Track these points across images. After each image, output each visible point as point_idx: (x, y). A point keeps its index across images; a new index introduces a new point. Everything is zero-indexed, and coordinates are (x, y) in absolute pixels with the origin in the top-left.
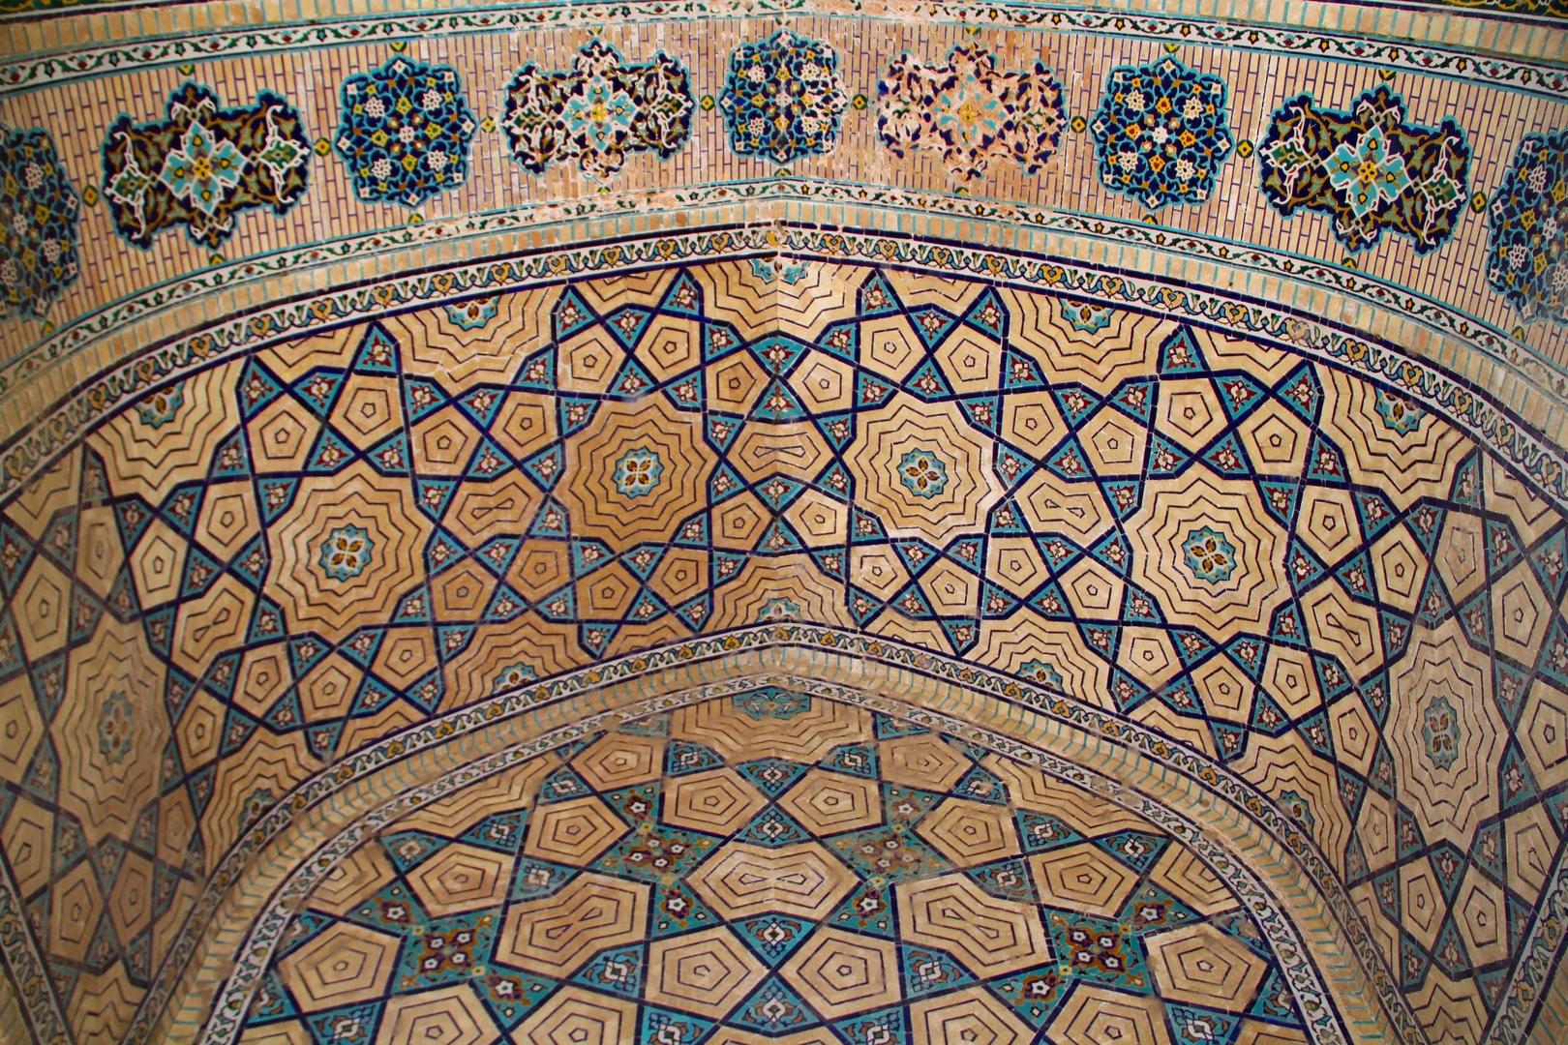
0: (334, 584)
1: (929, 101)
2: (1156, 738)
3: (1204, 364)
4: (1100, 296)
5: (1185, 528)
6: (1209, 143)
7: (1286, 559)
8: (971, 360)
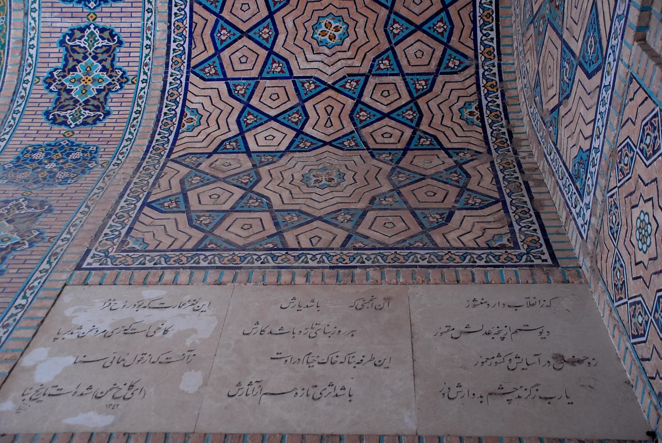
0: (347, 42)
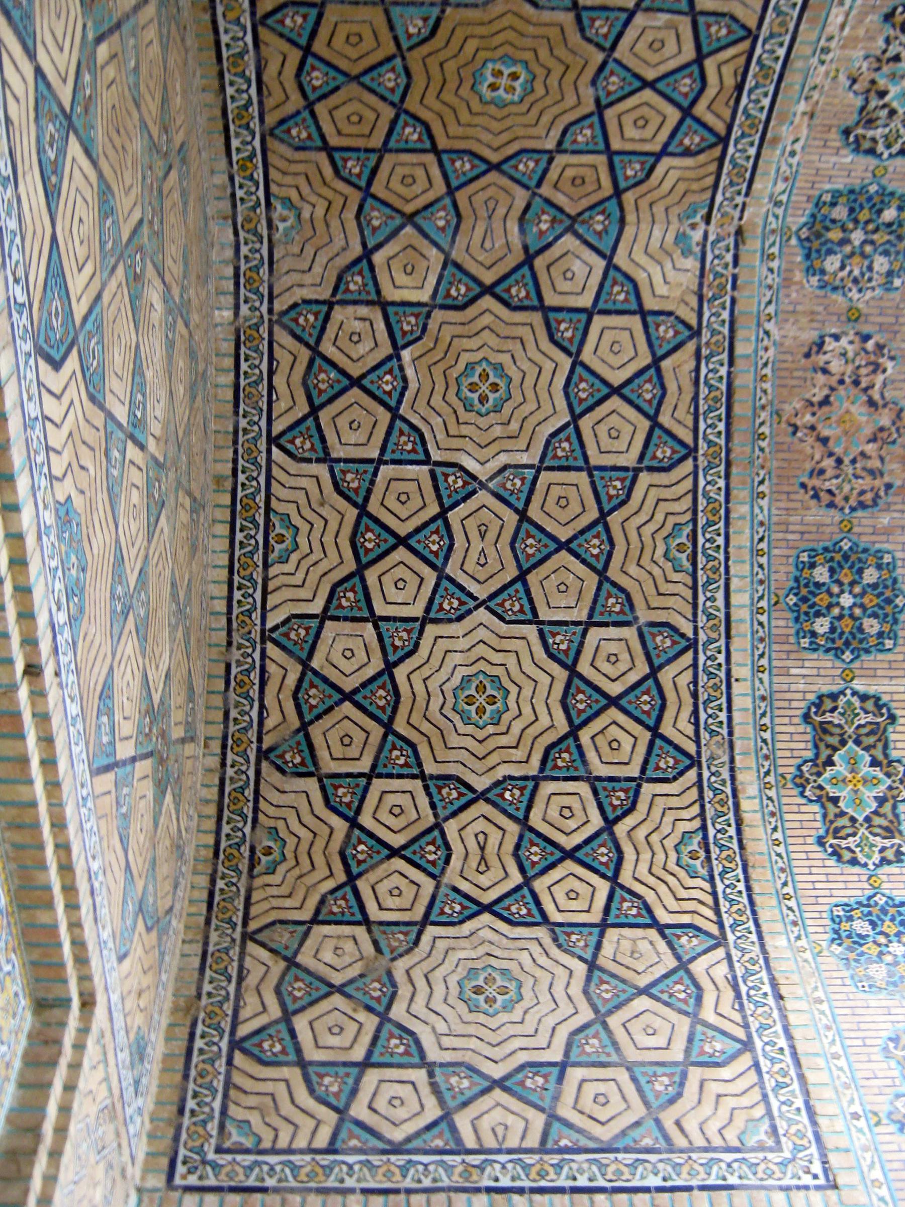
1: (856, 383)
2: (255, 676)
3: (661, 667)
4: (701, 560)
5: (499, 671)
6: (847, 643)
7: (511, 778)
8: (616, 435)
